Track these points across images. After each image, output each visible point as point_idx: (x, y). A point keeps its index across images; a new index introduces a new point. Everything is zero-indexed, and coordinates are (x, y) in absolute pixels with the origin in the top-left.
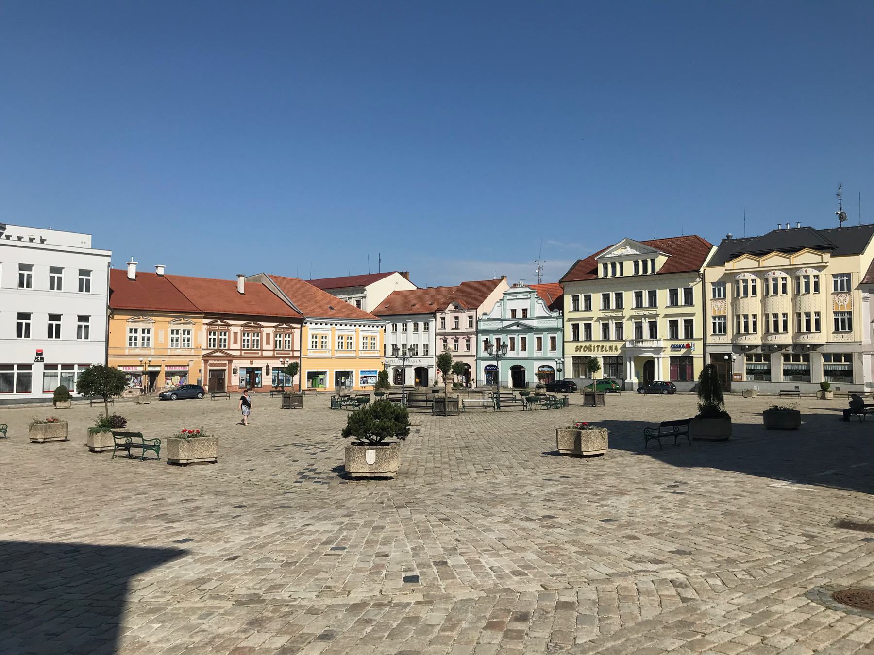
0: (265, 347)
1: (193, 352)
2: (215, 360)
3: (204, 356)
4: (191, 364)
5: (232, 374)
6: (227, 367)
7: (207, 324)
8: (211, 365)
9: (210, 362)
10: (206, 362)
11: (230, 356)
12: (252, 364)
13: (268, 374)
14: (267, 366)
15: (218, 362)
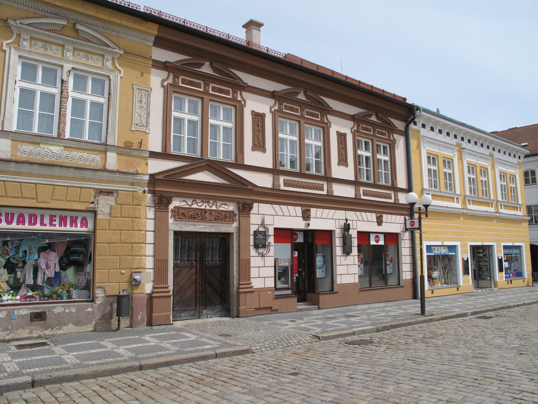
0: (337, 171)
2: (195, 197)
5: (253, 252)
6: (235, 225)
7: (164, 66)
8: (180, 214)
9: (176, 203)
12: (306, 216)
14: (346, 228)
15: (204, 206)
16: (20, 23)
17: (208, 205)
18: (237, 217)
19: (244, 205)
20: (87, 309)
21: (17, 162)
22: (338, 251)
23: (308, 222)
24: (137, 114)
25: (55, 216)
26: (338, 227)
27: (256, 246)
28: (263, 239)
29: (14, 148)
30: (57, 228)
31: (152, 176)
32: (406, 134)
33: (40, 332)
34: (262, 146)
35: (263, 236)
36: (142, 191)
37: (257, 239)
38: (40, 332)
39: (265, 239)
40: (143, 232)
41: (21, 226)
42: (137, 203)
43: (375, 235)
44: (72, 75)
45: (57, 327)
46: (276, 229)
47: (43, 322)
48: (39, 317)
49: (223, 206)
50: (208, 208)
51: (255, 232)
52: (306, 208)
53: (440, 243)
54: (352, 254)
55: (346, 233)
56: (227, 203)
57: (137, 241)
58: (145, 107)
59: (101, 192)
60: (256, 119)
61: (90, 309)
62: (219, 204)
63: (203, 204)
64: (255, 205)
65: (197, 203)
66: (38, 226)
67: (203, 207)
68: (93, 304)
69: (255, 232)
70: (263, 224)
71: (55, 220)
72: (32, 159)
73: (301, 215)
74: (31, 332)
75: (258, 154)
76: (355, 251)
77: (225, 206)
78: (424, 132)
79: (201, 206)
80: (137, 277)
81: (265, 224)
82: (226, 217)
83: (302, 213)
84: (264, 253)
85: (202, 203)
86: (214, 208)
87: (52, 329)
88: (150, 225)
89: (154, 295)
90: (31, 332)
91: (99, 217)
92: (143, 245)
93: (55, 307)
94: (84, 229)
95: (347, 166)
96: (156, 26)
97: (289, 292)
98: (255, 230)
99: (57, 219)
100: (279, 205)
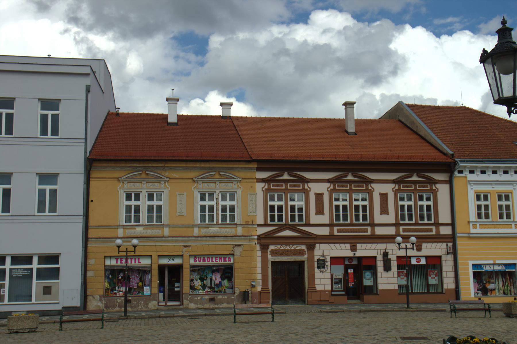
1: (240, 231)
2: (281, 244)
3: (260, 237)
4: (238, 252)
5: (316, 270)
6: (306, 256)
7: (263, 180)
8: (274, 253)
9: (272, 247)
10: (264, 248)
11: (309, 235)
13: (387, 268)
14: (385, 255)
15: (288, 248)
16: (198, 179)
17: (290, 247)
18: (307, 253)
19: (310, 245)
20: (231, 297)
21: (201, 237)
22: (380, 268)
23: (354, 252)
24: (250, 207)
25: (217, 258)
26: (379, 254)
27: (319, 267)
28: (323, 263)
29: (199, 231)
30: (218, 262)
31: (259, 236)
32: (450, 182)
33: (213, 306)
34: (322, 211)
35: (323, 262)
36: (254, 244)
37: (319, 263)
38: (213, 306)
39: (324, 264)
40: (256, 263)
41: (204, 263)
42: (253, 249)
43: (416, 258)
44: (220, 195)
45: (220, 304)
46: (331, 258)
47: (214, 302)
48: (212, 300)
49: (298, 247)
50: (289, 249)
51: (317, 260)
52: (353, 244)
53: (492, 262)
54: (392, 271)
55: (386, 258)
56: (300, 246)
57: (253, 267)
58: (254, 203)
59: (236, 245)
60: (317, 197)
61: (233, 297)
62: (295, 246)
63: (286, 247)
64: (317, 246)
65: (283, 247)
66: (211, 262)
67: (287, 249)
68: (234, 295)
69: (317, 260)
70: (323, 256)
71: (217, 259)
72: (207, 234)
73: (350, 249)
74: (210, 306)
75: (320, 217)
76: (394, 268)
77: (299, 247)
78: (471, 177)
79: (285, 248)
80: (253, 283)
81: (324, 255)
82: (300, 253)
83: (351, 248)
84: (324, 271)
85: (286, 247)
86: (293, 248)
87: (218, 305)
88: (259, 259)
89: (262, 292)
90: (210, 306)
91: (235, 257)
92: (256, 269)
93: (218, 296)
94: (229, 262)
95: (388, 214)
96: (256, 163)
97: (344, 293)
98: (318, 259)
99: (218, 259)
100: (334, 244)
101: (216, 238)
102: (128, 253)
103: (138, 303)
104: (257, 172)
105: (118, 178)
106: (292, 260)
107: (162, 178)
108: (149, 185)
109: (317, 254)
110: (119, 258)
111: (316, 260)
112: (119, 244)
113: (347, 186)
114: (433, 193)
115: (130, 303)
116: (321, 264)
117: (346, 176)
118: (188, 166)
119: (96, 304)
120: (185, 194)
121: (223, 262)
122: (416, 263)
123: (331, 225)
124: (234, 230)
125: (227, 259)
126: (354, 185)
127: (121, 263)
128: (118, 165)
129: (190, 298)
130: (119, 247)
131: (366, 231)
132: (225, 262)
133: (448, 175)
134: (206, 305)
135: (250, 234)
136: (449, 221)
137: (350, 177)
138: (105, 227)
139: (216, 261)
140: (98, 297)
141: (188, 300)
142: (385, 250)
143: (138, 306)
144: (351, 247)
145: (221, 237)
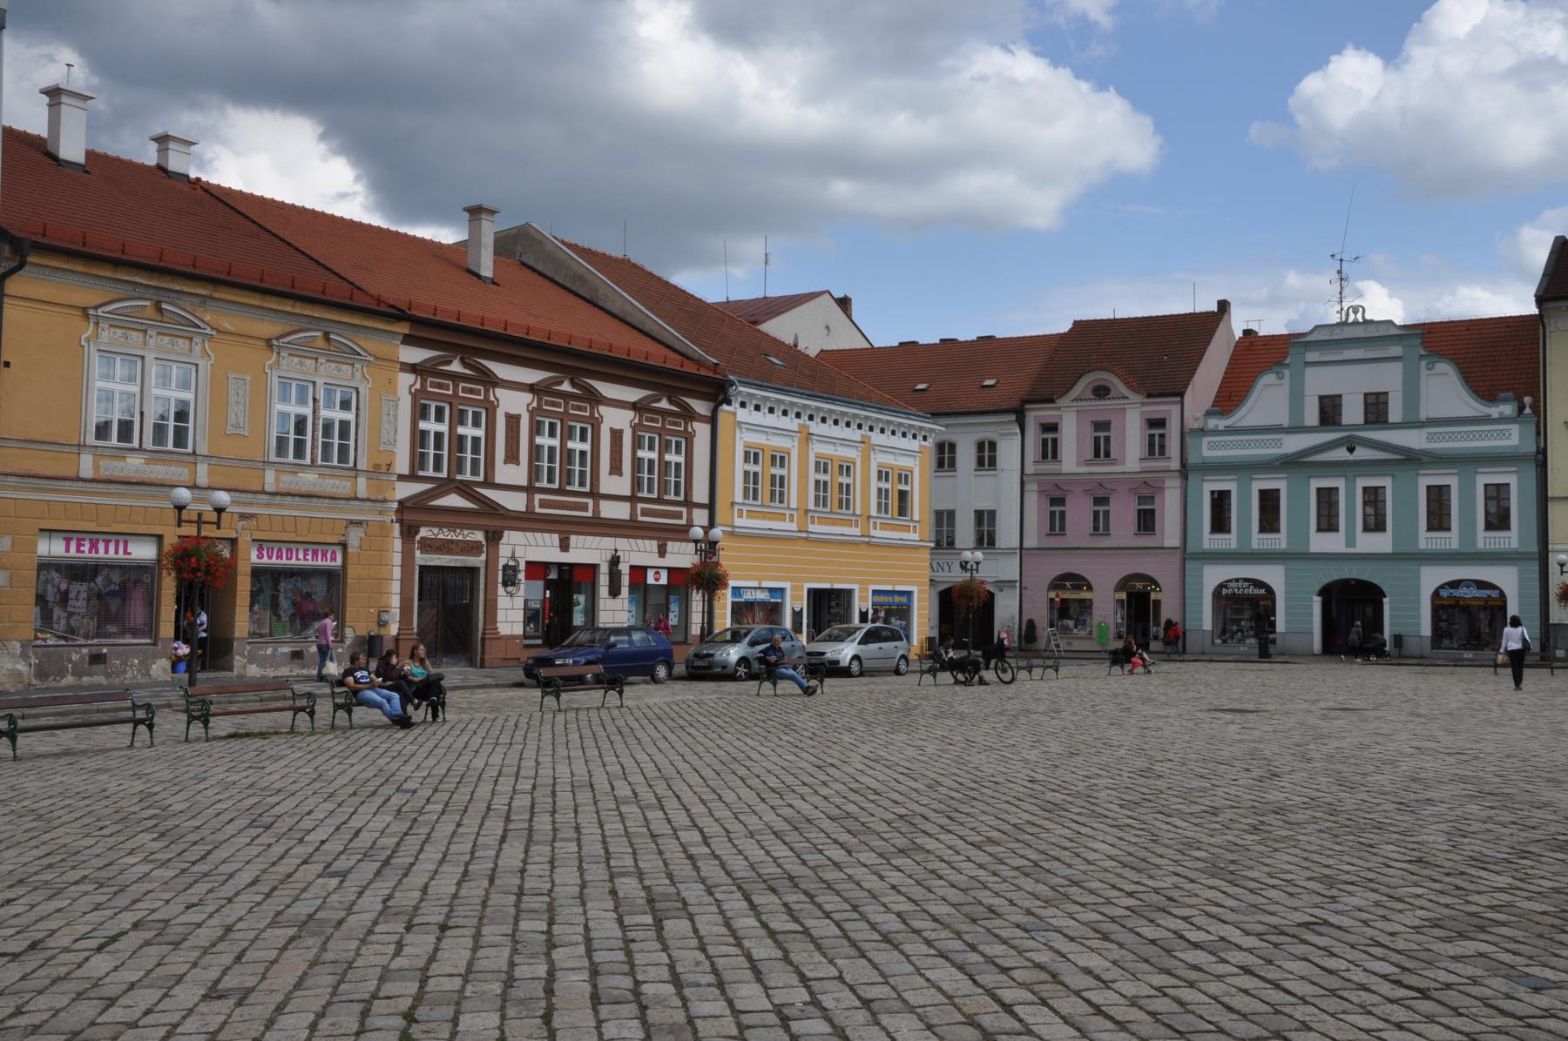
1: (362, 487)
2: (440, 525)
6: (483, 557)
7: (413, 368)
8: (428, 546)
9: (424, 532)
10: (409, 532)
11: (493, 509)
12: (564, 546)
13: (614, 592)
14: (615, 561)
15: (451, 536)
19: (494, 532)
21: (282, 494)
22: (603, 591)
27: (505, 584)
30: (310, 562)
31: (401, 502)
32: (713, 421)
39: (515, 576)
41: (279, 561)
43: (654, 570)
59: (352, 522)
62: (466, 532)
64: (506, 533)
66: (293, 561)
70: (513, 558)
75: (511, 467)
76: (625, 591)
78: (744, 415)
86: (460, 538)
88: (397, 559)
94: (333, 563)
95: (621, 475)
97: (539, 642)
99: (310, 553)
101: (315, 500)
102: (204, 526)
103: (124, 663)
104: (402, 346)
105: (85, 310)
106: (458, 565)
107: (199, 327)
108: (115, 333)
109: (504, 553)
110: (75, 536)
111: (501, 568)
112: (182, 502)
113: (478, 393)
114: (487, 409)
115: (105, 663)
116: (510, 580)
117: (449, 363)
118: (266, 305)
119: (10, 666)
120: (249, 378)
121: (320, 562)
122: (654, 582)
123: (632, 499)
124: (349, 484)
125: (329, 555)
126: (432, 383)
127: (78, 551)
128: (94, 271)
129: (249, 652)
130: (180, 508)
131: (584, 508)
132: (324, 563)
133: (712, 405)
134: (283, 669)
135: (380, 497)
136: (706, 501)
137: (456, 367)
138: (46, 447)
139: (305, 559)
140: (17, 647)
141: (244, 657)
142: (616, 551)
143: (125, 672)
144: (561, 540)
145: (325, 498)
